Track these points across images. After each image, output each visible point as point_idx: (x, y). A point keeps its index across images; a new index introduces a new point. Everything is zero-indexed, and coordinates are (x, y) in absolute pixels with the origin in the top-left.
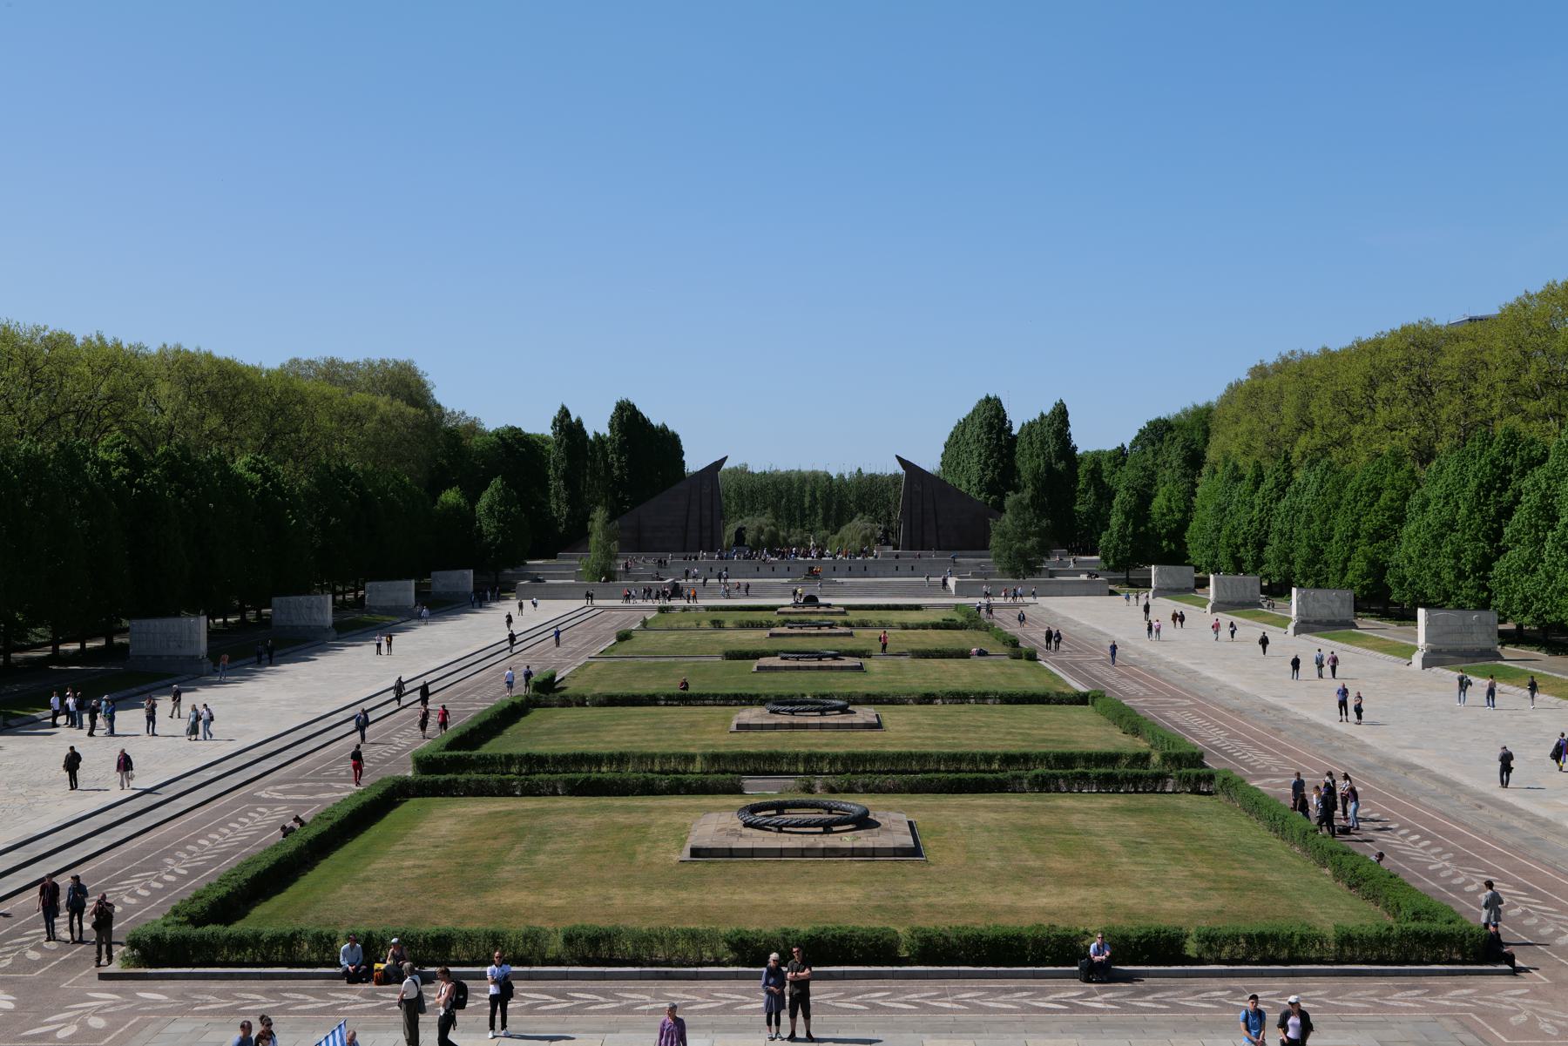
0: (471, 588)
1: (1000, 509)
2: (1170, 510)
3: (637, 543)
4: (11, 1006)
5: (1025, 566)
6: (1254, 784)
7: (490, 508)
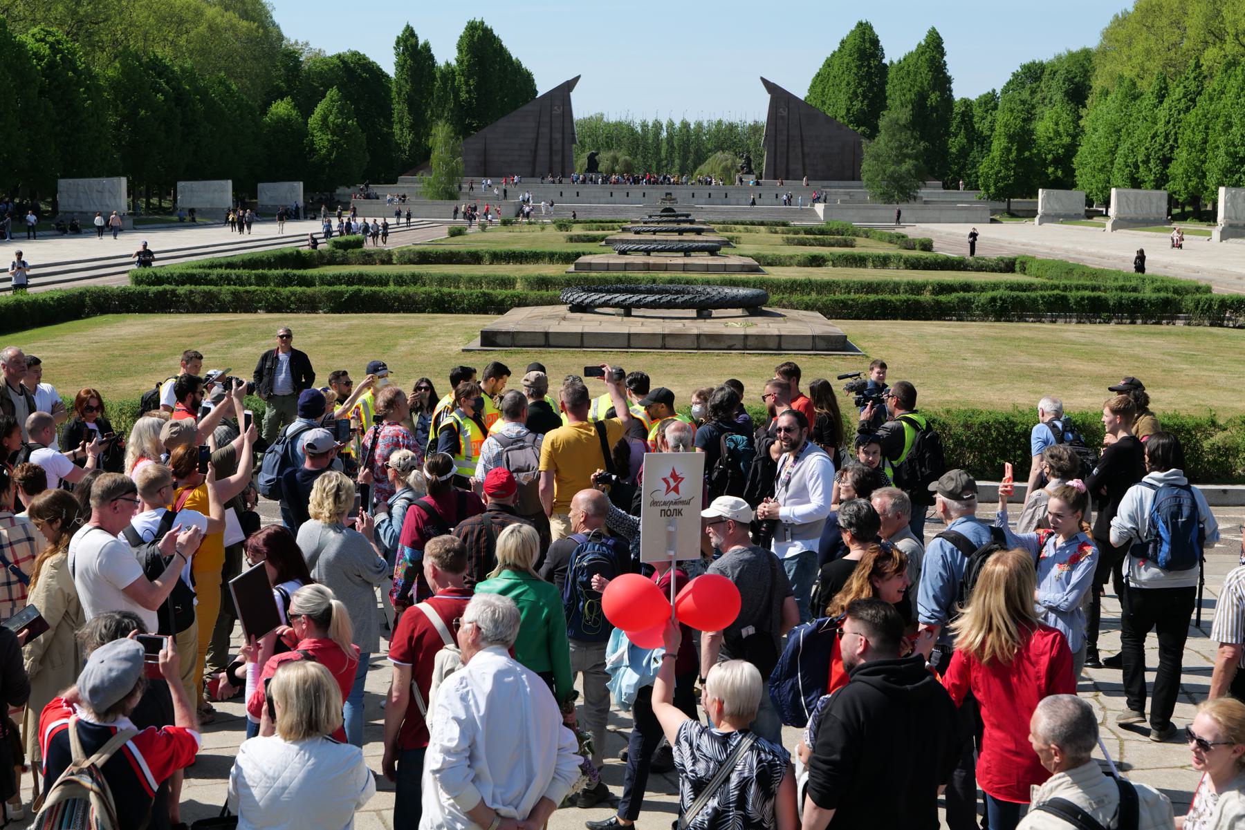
0: (301, 203)
1: (873, 132)
2: (1057, 133)
3: (485, 169)
5: (900, 191)
7: (324, 119)
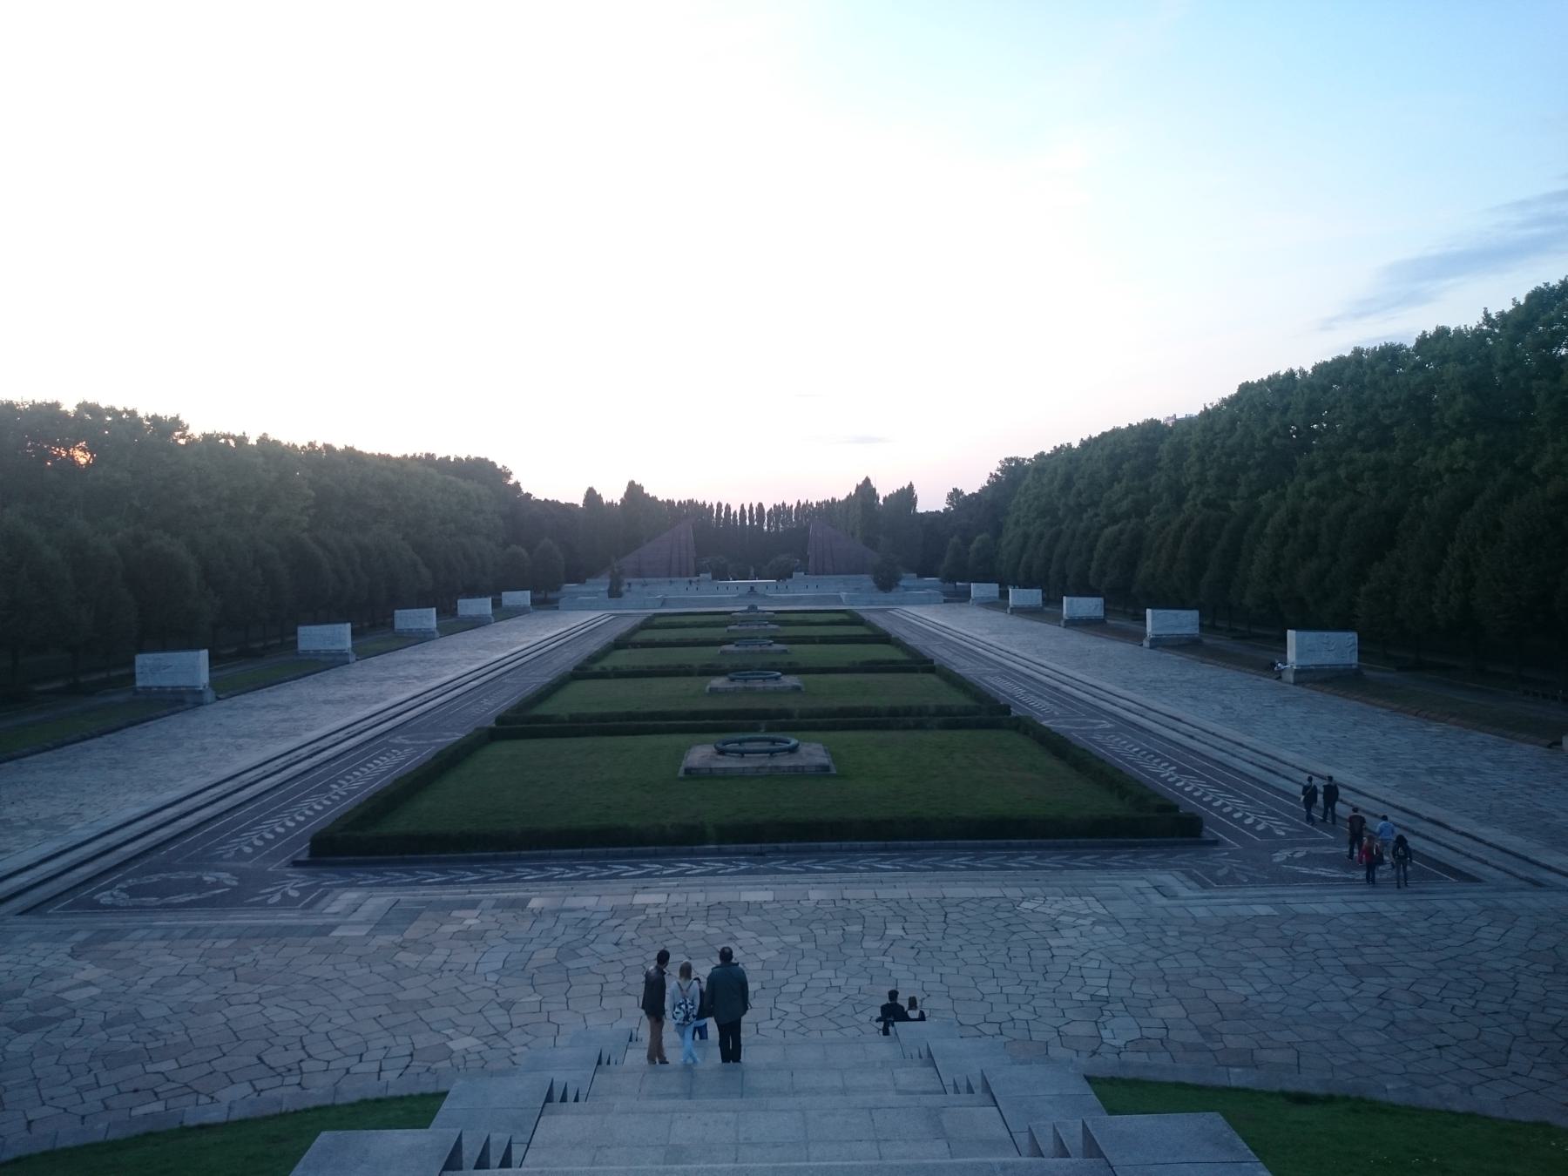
4: (235, 883)
6: (1045, 723)
